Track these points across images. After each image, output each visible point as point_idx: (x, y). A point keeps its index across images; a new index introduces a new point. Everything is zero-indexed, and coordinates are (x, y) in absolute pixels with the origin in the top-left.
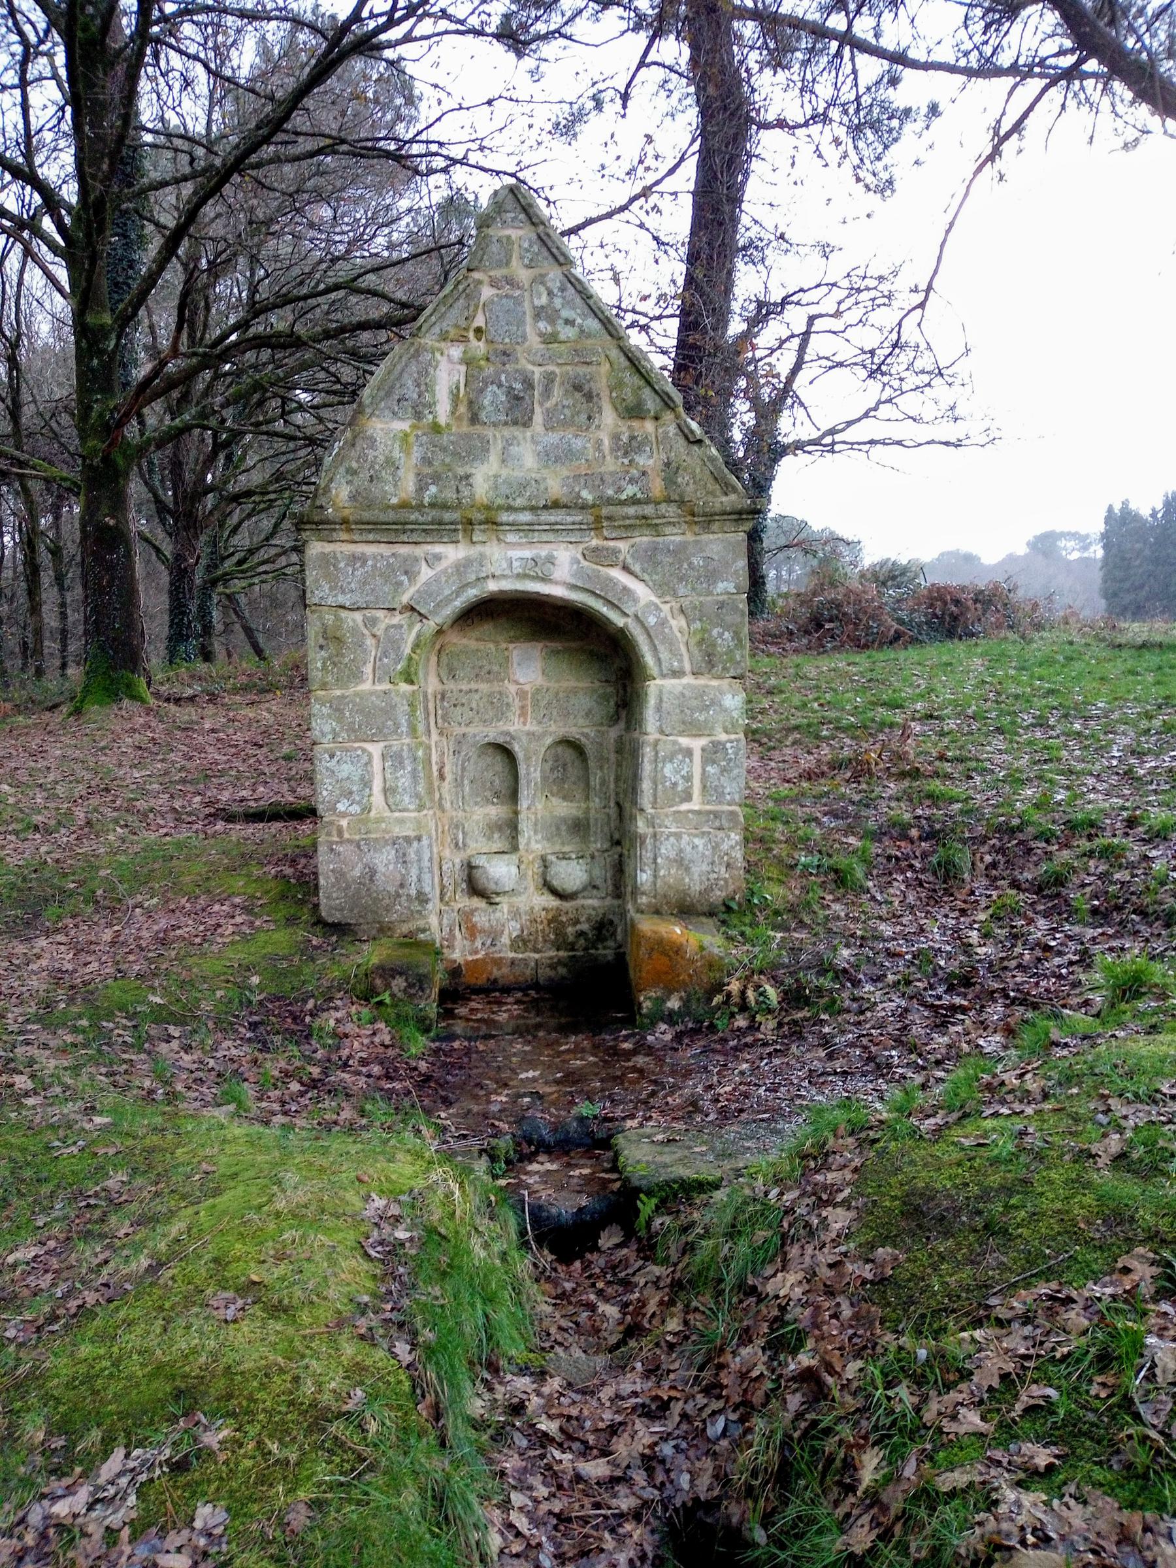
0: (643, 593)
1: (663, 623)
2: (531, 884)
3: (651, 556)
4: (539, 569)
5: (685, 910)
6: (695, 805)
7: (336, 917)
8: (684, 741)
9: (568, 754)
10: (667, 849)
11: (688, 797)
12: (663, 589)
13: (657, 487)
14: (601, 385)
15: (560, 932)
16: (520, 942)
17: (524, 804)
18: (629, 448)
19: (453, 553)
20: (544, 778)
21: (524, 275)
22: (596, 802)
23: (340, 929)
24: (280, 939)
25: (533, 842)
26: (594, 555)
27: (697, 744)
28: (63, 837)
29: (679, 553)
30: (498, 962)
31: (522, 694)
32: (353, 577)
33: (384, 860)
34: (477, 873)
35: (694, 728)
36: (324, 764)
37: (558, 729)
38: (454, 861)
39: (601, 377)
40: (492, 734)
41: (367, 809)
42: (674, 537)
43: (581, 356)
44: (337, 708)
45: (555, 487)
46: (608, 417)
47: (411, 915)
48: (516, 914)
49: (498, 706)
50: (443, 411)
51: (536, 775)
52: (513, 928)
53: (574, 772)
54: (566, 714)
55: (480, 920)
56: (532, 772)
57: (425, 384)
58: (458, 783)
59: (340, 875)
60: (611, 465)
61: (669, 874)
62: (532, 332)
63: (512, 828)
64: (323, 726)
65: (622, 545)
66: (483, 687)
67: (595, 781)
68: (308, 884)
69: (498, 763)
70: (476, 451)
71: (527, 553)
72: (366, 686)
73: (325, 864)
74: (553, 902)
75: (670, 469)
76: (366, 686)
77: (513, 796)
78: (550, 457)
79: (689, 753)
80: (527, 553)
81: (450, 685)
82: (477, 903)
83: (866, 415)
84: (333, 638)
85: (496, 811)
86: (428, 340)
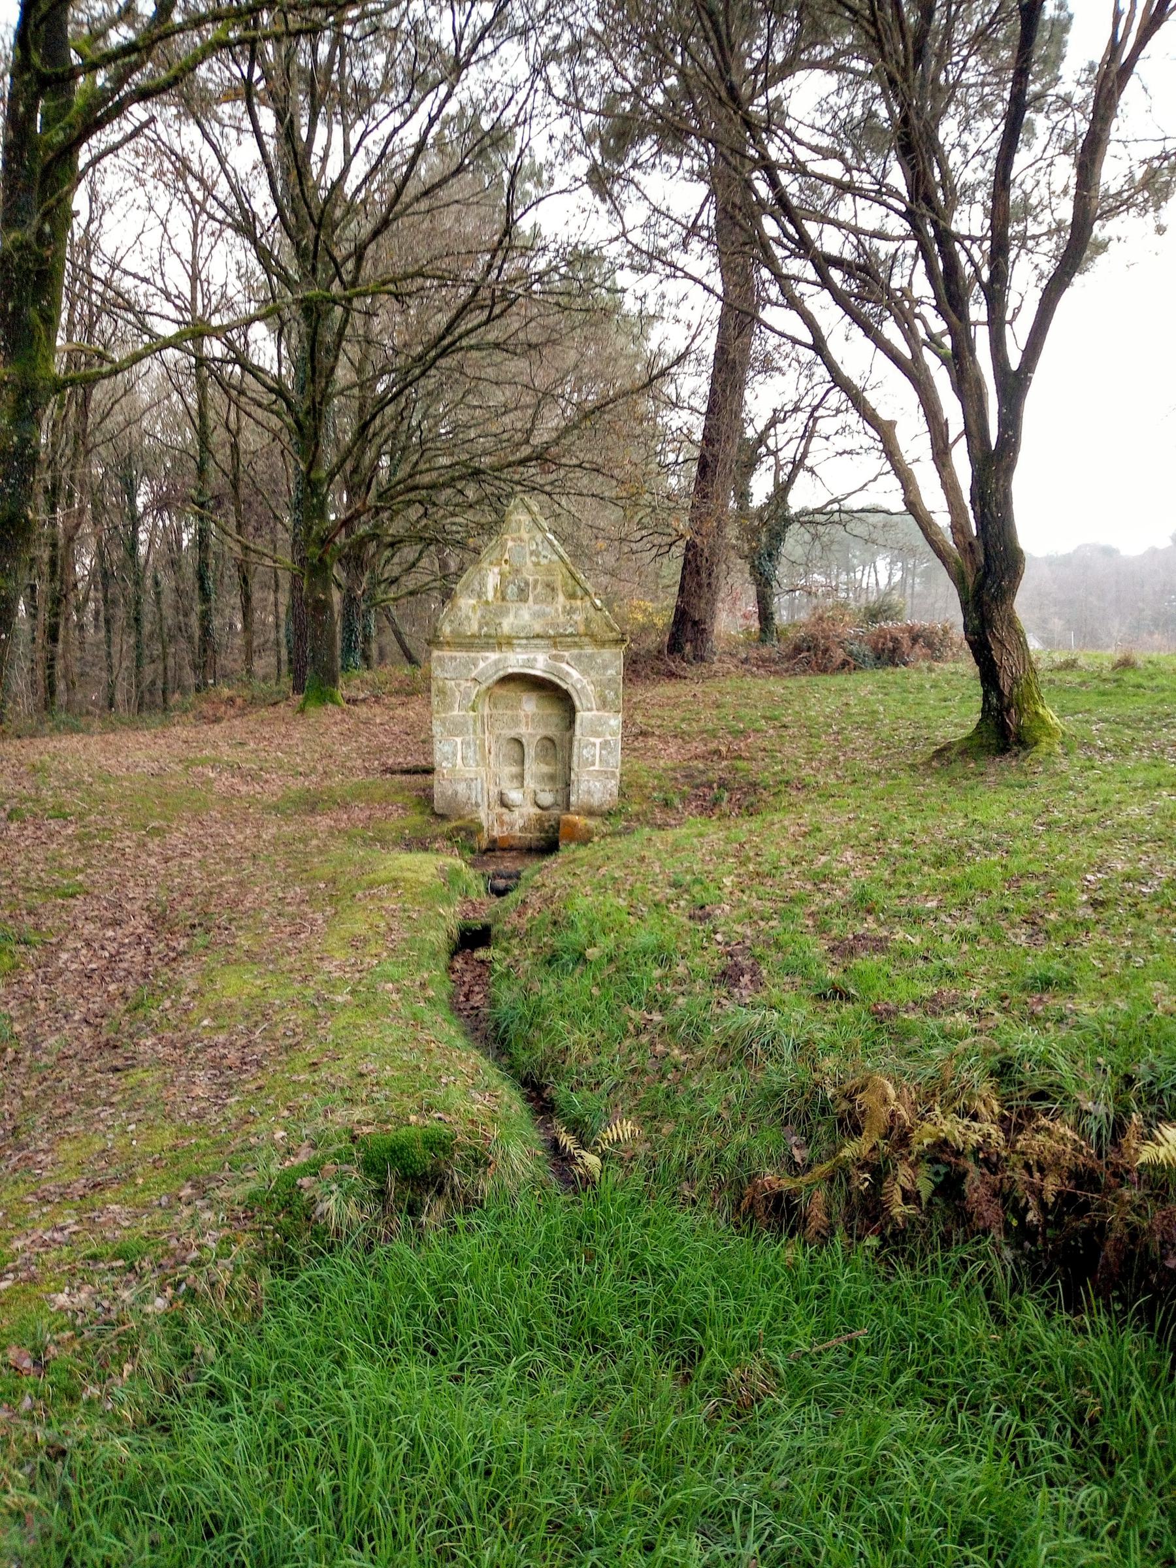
0: (575, 674)
1: (583, 687)
2: (529, 802)
3: (578, 658)
4: (530, 663)
5: (591, 813)
6: (597, 767)
7: (440, 811)
8: (592, 739)
9: (548, 744)
10: (583, 787)
11: (593, 764)
12: (584, 672)
13: (582, 629)
14: (558, 584)
15: (541, 825)
16: (523, 829)
17: (526, 766)
18: (570, 612)
19: (493, 656)
20: (537, 755)
21: (526, 536)
22: (560, 766)
23: (442, 817)
24: (416, 819)
25: (530, 783)
26: (555, 658)
27: (598, 741)
28: (314, 778)
29: (591, 657)
30: (514, 838)
31: (527, 716)
32: (450, 666)
33: (461, 788)
34: (505, 798)
35: (597, 734)
36: (437, 746)
37: (542, 732)
38: (494, 791)
39: (558, 581)
40: (513, 733)
41: (454, 766)
42: (589, 650)
43: (549, 571)
44: (443, 723)
45: (538, 628)
46: (561, 598)
47: (472, 812)
48: (522, 816)
49: (516, 722)
50: (490, 595)
51: (533, 753)
52: (520, 823)
53: (551, 752)
54: (546, 725)
55: (506, 818)
56: (531, 751)
57: (483, 584)
58: (497, 756)
59: (443, 793)
60: (562, 619)
61: (584, 798)
62: (529, 561)
63: (521, 777)
64: (437, 729)
65: (566, 654)
66: (509, 712)
67: (560, 756)
68: (430, 799)
69: (517, 747)
70: (503, 612)
71: (525, 657)
72: (456, 713)
73: (437, 789)
74: (539, 811)
75: (588, 622)
76: (456, 713)
77: (522, 762)
78: (536, 615)
79: (594, 745)
80: (525, 657)
81: (494, 711)
82: (504, 810)
83: (861, 489)
84: (442, 692)
85: (515, 769)
86: (485, 565)
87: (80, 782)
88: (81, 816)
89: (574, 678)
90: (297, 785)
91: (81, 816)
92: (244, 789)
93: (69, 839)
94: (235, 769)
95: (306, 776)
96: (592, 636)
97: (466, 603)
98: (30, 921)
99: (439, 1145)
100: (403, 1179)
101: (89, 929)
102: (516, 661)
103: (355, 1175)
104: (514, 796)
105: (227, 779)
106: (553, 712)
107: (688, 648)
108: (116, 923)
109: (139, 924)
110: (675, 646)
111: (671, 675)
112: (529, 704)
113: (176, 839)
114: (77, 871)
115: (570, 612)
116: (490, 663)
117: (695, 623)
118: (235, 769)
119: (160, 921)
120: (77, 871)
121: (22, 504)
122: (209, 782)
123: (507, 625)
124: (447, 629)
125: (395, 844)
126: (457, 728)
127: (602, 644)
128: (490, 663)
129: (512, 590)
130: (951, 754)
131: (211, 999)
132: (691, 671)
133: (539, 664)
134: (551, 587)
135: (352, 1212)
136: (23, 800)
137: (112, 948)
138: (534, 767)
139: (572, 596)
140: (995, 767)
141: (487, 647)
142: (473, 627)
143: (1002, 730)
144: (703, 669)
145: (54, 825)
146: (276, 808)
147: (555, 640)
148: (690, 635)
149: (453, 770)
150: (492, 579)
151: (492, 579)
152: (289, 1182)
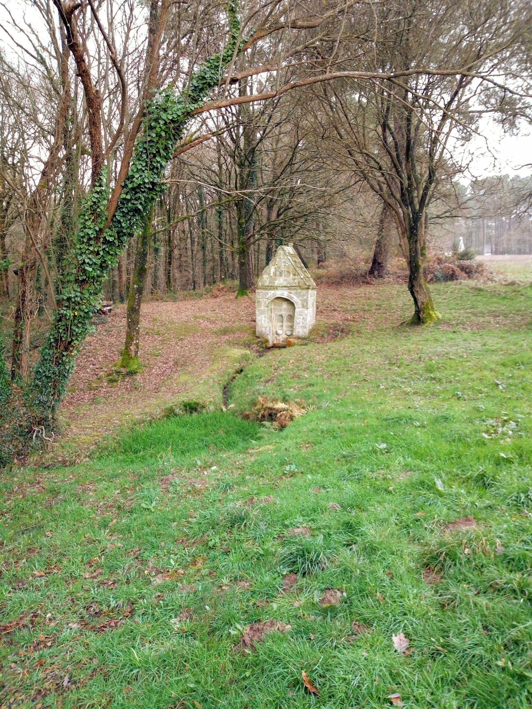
0: (295, 298)
3: (296, 293)
4: (283, 294)
5: (299, 338)
10: (297, 330)
12: (298, 297)
13: (297, 284)
14: (291, 272)
16: (283, 341)
18: (294, 279)
19: (273, 292)
21: (282, 257)
23: (258, 337)
24: (251, 337)
25: (285, 328)
26: (290, 293)
27: (301, 317)
28: (230, 323)
29: (300, 293)
32: (261, 294)
33: (263, 329)
35: (301, 315)
36: (257, 317)
37: (288, 313)
38: (274, 330)
39: (291, 270)
40: (280, 313)
42: (299, 291)
43: (288, 267)
44: (259, 310)
45: (285, 284)
46: (292, 276)
49: (281, 310)
50: (272, 274)
52: (282, 340)
56: (285, 319)
57: (270, 271)
60: (292, 281)
61: (297, 333)
62: (283, 264)
63: (282, 326)
64: (257, 312)
68: (254, 332)
70: (275, 279)
73: (257, 330)
75: (299, 282)
77: (282, 322)
78: (285, 280)
84: (259, 302)
85: (281, 324)
86: (270, 265)
87: (165, 324)
88: (163, 335)
89: (295, 299)
90: (224, 325)
91: (163, 335)
92: (209, 326)
93: (159, 341)
94: (208, 320)
95: (228, 322)
96: (300, 287)
97: (265, 276)
98: (147, 362)
99: (197, 404)
100: (190, 408)
101: (160, 364)
102: (279, 293)
103: (182, 407)
104: (280, 332)
105: (206, 323)
106: (291, 307)
107: (376, 272)
108: (166, 363)
109: (171, 364)
110: (371, 272)
111: (368, 283)
112: (285, 305)
113: (186, 342)
114: (160, 350)
115: (294, 279)
116: (271, 294)
117: (379, 264)
118: (208, 320)
119: (176, 363)
120: (160, 350)
121: (144, 265)
122: (200, 324)
123: (276, 283)
124: (260, 284)
125: (242, 345)
126: (263, 312)
127: (303, 289)
128: (271, 294)
129: (278, 273)
130: (404, 325)
131: (178, 381)
132: (375, 281)
133: (285, 294)
134: (288, 272)
135: (181, 412)
136: (150, 329)
137: (164, 369)
138: (285, 323)
139: (294, 275)
140: (419, 329)
141: (270, 289)
142: (267, 284)
143: (419, 318)
144: (381, 280)
145: (156, 337)
146: (216, 333)
147: (289, 287)
148: (377, 268)
149: (261, 324)
150: (273, 270)
151: (273, 270)
152: (172, 407)
